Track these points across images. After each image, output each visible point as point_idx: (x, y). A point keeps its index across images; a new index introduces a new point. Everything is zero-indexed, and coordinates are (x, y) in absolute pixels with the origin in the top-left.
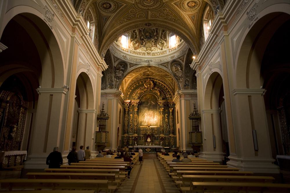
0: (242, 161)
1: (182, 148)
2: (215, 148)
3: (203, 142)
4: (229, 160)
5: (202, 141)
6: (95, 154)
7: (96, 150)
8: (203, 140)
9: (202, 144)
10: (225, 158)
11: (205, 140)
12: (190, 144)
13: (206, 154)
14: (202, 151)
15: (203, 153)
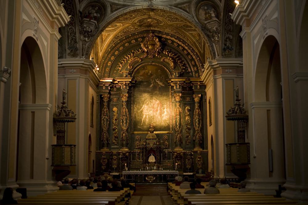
0: (302, 191)
1: (218, 174)
2: (271, 172)
3: (251, 162)
4: (285, 189)
5: (249, 161)
6: (52, 186)
7: (53, 180)
8: (252, 157)
9: (249, 165)
10: (280, 186)
11: (255, 157)
12: (231, 167)
13: (255, 183)
14: (250, 178)
15: (251, 181)
